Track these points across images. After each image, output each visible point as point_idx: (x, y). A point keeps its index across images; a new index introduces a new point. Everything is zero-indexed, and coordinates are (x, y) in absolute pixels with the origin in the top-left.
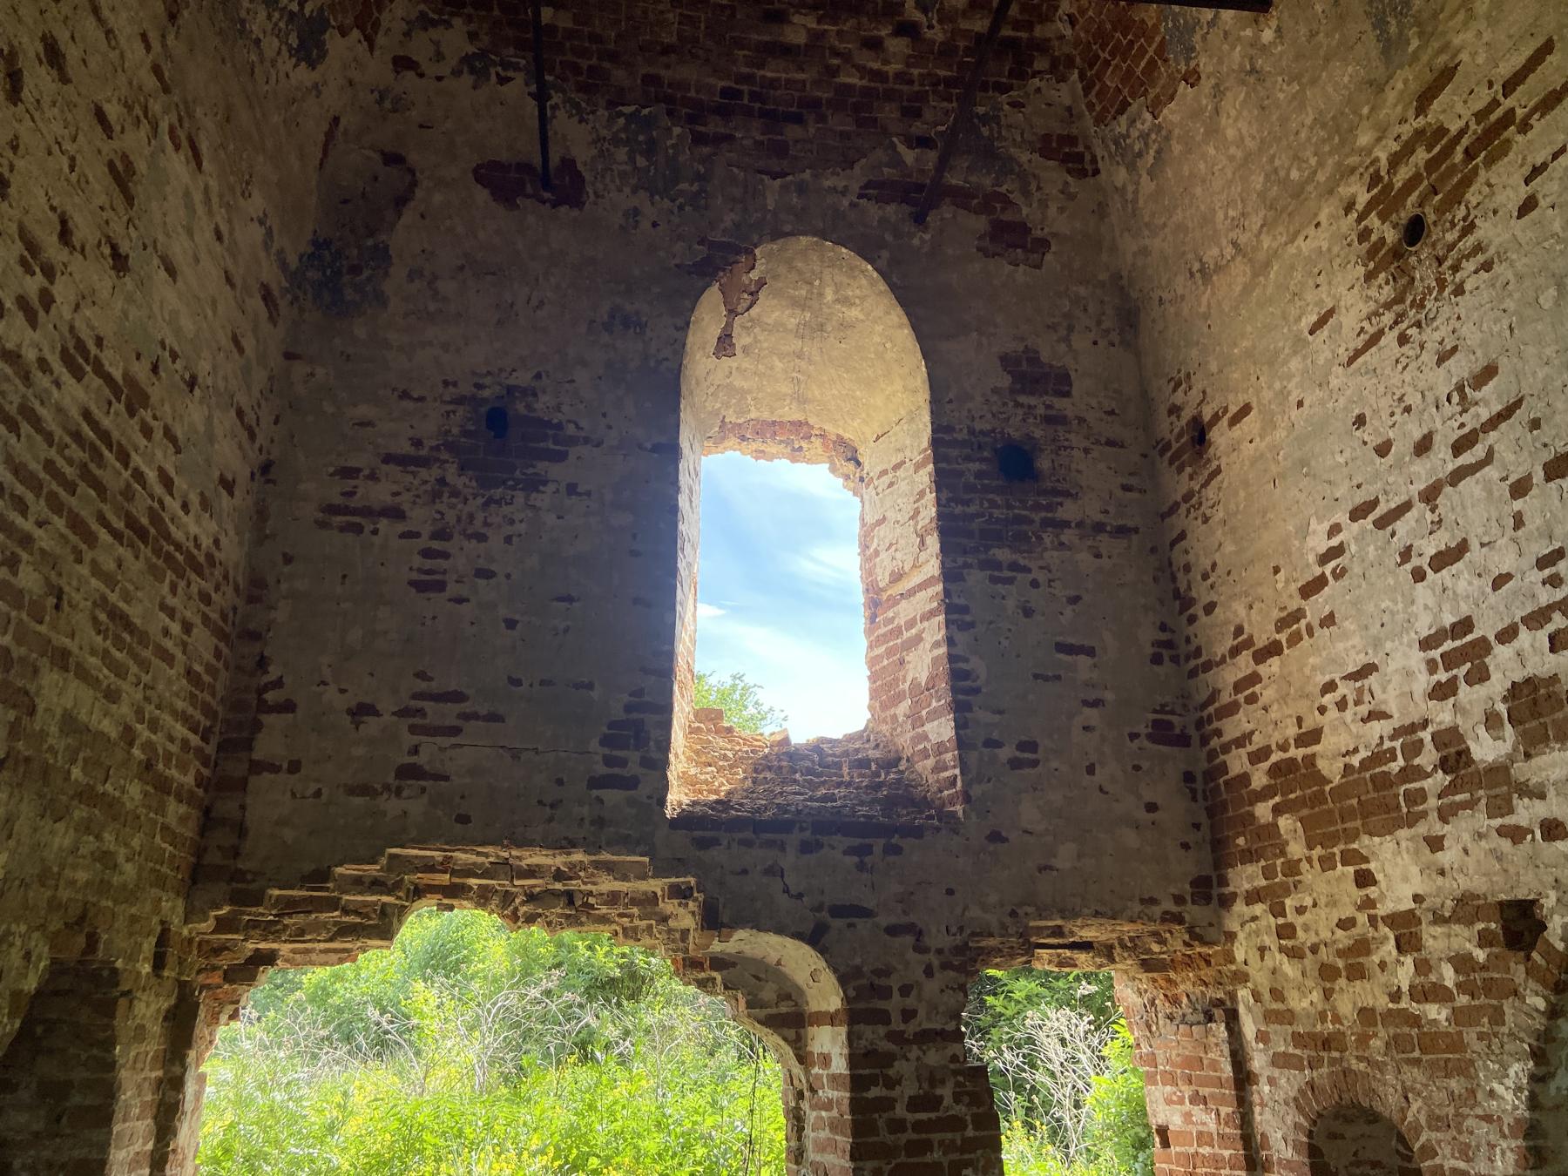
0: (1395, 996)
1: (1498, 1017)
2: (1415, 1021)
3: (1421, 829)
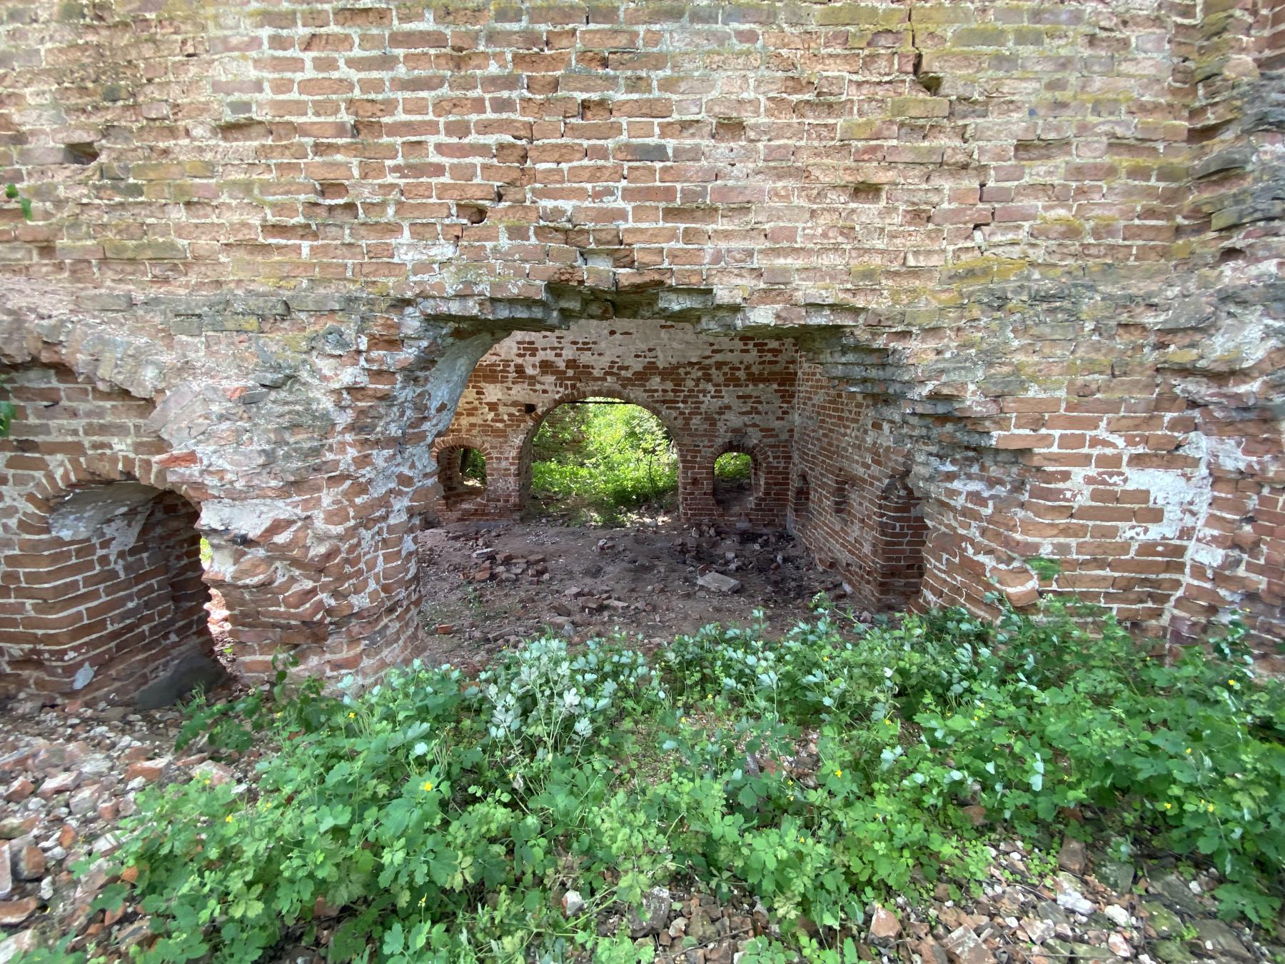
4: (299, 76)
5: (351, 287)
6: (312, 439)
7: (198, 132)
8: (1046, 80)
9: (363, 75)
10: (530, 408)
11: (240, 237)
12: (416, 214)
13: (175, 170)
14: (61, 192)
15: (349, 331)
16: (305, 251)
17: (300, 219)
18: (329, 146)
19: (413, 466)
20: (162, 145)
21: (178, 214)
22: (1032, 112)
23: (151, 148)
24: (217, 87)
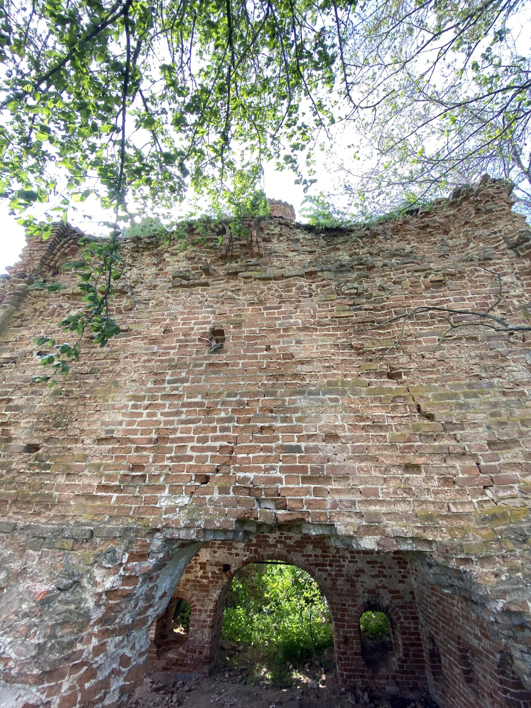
0: (196, 577)
1: (217, 582)
2: (199, 582)
3: (213, 549)
4: (139, 419)
5: (130, 521)
6: (72, 633)
7: (87, 441)
8: (488, 412)
9: (166, 419)
10: (226, 568)
11: (85, 491)
12: (175, 480)
13: (69, 458)
14: (13, 466)
15: (119, 550)
16: (114, 499)
17: (117, 483)
18: (143, 448)
19: (133, 648)
20: (69, 446)
21: (62, 480)
22: (489, 428)
23: (64, 448)
24: (103, 423)
